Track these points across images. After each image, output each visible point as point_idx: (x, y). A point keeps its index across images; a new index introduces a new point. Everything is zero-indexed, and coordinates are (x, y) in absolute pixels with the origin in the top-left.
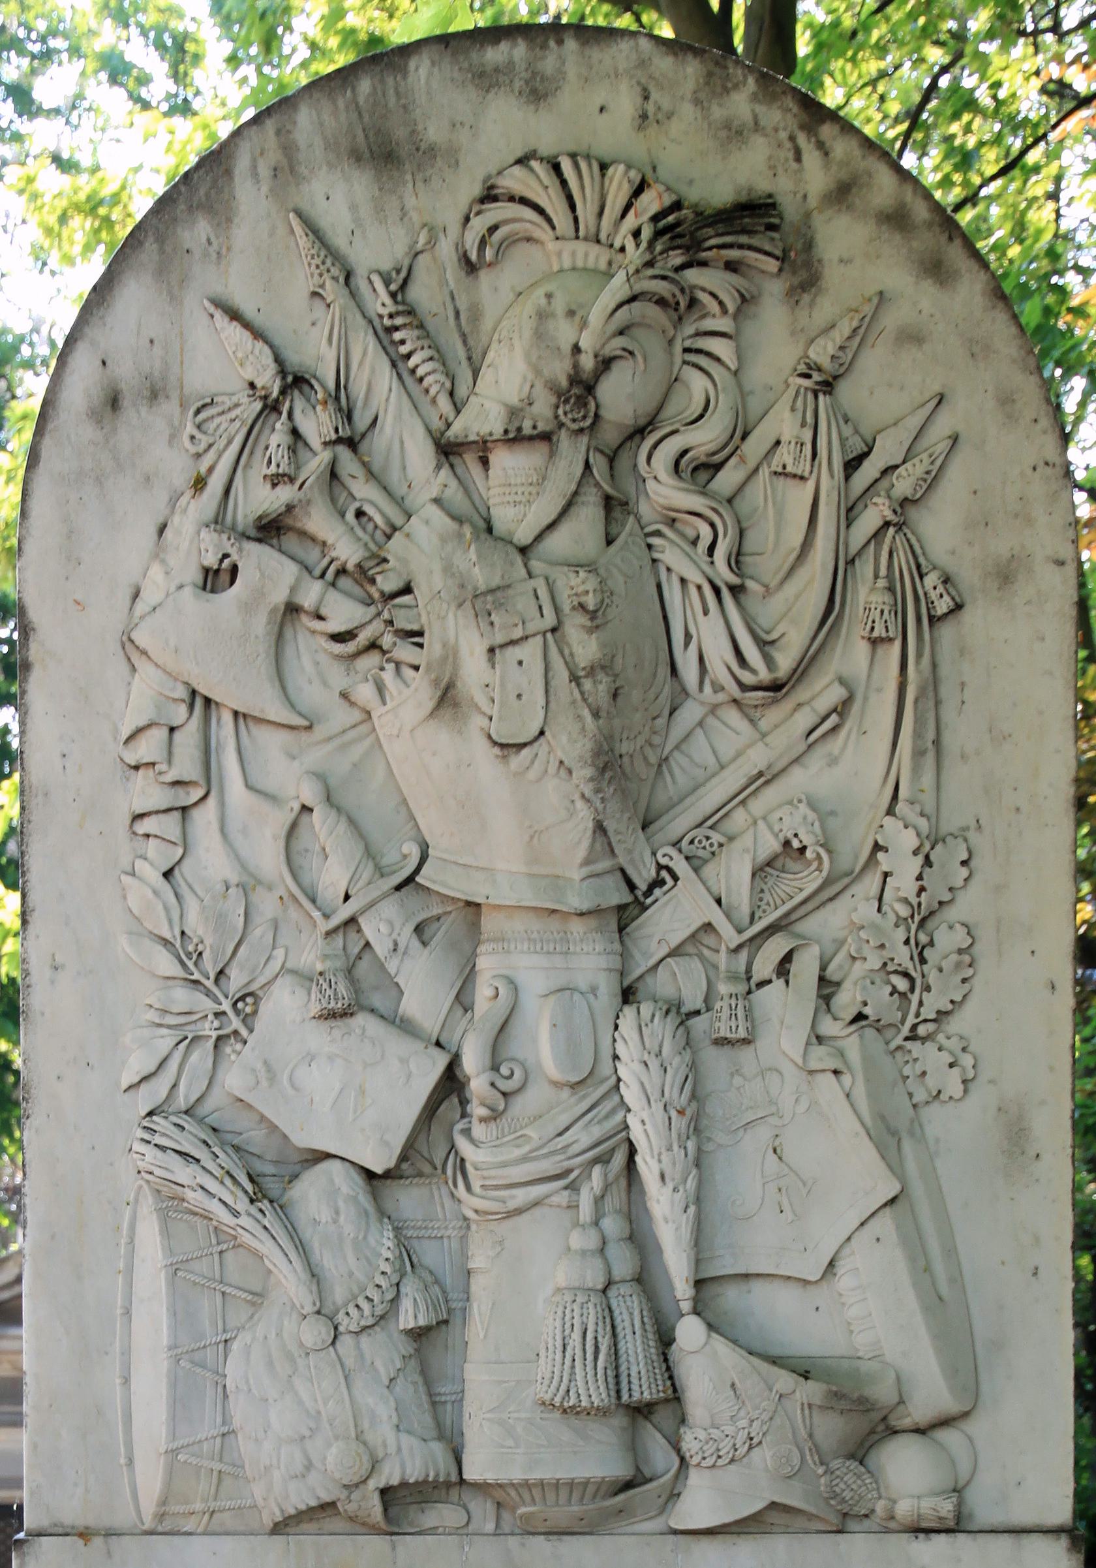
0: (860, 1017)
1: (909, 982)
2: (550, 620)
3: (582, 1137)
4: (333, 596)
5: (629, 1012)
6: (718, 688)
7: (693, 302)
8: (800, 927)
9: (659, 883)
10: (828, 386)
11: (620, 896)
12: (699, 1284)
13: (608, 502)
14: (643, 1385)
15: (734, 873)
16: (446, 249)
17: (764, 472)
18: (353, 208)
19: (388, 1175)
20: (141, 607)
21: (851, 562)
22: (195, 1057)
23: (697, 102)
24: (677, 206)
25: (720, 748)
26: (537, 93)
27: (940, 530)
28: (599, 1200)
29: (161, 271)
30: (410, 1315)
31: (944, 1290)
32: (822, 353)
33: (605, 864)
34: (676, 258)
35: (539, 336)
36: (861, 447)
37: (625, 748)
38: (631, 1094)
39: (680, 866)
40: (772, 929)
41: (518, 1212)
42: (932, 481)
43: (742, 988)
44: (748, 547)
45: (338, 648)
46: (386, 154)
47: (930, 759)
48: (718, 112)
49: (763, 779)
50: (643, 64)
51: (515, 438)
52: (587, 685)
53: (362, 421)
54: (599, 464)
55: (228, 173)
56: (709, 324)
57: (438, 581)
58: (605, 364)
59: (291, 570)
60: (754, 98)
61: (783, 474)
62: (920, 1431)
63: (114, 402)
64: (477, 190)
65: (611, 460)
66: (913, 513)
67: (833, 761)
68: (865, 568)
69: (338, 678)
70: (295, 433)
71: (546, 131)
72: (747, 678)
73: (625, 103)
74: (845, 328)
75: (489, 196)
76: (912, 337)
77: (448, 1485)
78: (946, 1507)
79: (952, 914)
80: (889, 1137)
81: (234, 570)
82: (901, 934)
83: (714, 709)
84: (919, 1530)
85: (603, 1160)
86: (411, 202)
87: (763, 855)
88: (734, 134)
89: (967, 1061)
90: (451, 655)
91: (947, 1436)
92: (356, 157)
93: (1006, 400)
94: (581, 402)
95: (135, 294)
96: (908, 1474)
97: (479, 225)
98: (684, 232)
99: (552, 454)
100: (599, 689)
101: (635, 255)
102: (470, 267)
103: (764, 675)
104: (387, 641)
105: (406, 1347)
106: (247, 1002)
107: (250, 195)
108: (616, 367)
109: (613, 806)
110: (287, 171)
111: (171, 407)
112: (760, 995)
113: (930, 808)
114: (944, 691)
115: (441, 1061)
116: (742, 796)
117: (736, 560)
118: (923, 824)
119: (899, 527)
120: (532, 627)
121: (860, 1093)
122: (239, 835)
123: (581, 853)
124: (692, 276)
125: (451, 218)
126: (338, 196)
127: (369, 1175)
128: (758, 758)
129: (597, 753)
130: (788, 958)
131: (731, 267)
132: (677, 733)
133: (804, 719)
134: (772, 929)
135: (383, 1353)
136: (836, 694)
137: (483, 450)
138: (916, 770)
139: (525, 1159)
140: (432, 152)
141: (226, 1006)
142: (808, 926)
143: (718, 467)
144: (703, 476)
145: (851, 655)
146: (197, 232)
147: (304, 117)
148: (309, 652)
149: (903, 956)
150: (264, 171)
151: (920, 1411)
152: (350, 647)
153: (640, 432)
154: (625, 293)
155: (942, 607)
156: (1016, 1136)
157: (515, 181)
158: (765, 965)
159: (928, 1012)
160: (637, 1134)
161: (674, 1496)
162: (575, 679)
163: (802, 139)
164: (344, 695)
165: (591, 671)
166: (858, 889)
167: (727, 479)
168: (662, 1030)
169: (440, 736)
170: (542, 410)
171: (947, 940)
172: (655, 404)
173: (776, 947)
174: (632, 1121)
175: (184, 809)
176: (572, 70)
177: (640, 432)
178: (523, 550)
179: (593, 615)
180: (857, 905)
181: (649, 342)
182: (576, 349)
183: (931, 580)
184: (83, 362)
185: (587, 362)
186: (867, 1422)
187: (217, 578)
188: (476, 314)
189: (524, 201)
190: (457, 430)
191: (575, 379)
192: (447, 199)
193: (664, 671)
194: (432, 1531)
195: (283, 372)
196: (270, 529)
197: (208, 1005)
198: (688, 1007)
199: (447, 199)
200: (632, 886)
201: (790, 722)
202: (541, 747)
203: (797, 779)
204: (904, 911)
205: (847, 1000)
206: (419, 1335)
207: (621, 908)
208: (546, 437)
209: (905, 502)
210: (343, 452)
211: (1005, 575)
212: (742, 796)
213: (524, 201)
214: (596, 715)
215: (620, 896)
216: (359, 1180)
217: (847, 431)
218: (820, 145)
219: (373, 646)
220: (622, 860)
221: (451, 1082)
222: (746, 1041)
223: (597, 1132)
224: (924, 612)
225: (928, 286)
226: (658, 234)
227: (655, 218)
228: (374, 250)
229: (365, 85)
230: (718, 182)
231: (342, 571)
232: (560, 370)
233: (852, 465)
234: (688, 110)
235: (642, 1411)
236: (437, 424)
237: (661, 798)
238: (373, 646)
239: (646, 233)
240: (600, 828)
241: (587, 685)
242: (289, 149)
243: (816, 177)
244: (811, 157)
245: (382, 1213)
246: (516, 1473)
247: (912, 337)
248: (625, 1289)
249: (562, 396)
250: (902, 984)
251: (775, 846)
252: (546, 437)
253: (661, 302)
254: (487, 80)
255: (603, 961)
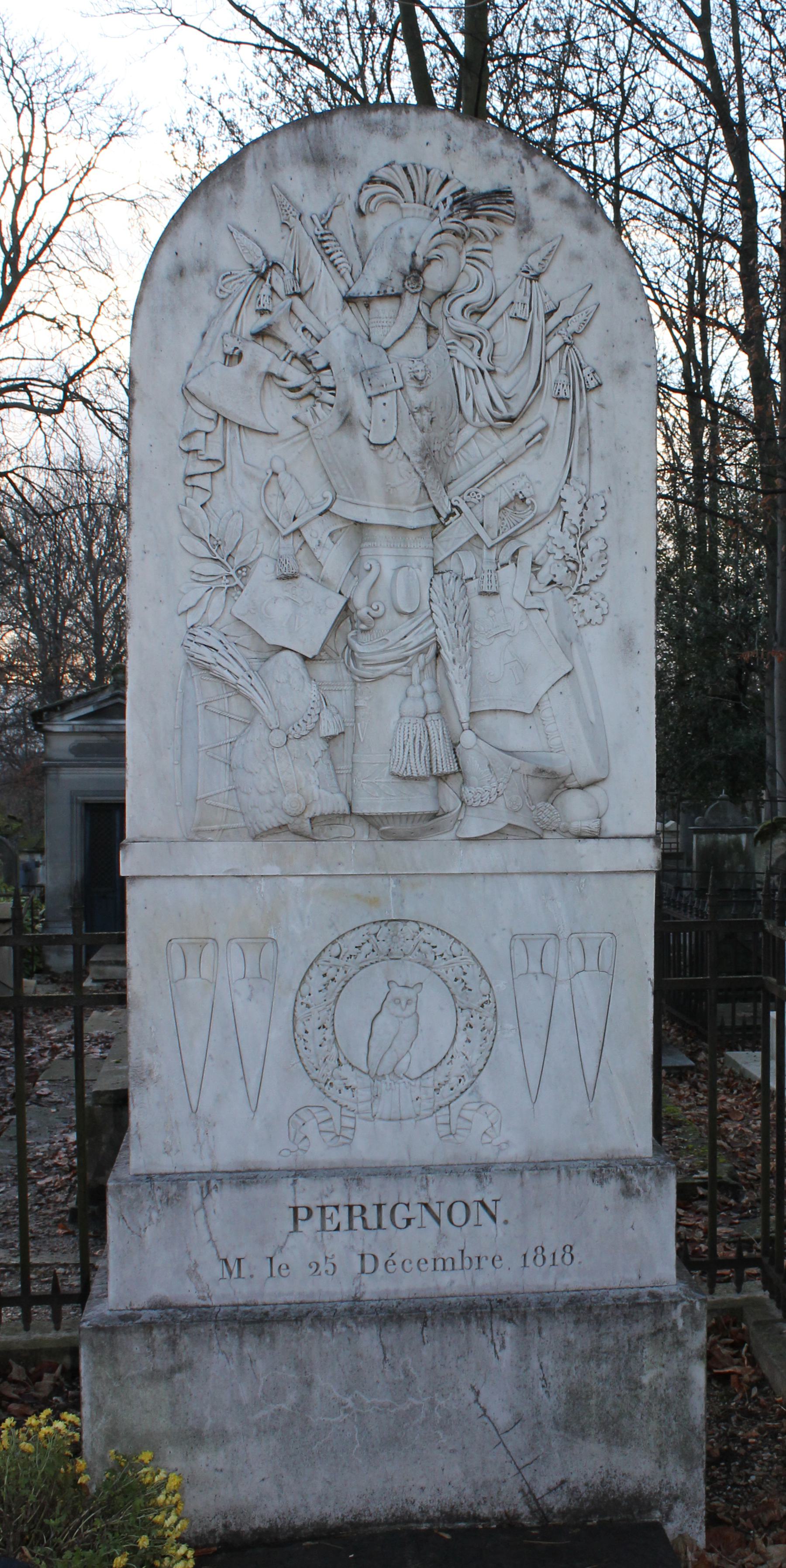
0: (552, 582)
1: (575, 565)
2: (400, 384)
3: (413, 640)
4: (290, 368)
5: (438, 578)
6: (482, 418)
7: (471, 235)
8: (522, 538)
9: (454, 514)
10: (537, 277)
11: (432, 520)
12: (472, 714)
13: (429, 328)
14: (446, 766)
15: (491, 510)
16: (349, 206)
17: (506, 317)
18: (304, 184)
19: (314, 659)
20: (192, 372)
21: (547, 361)
22: (215, 600)
23: (474, 143)
24: (464, 190)
25: (479, 449)
26: (396, 134)
27: (589, 348)
28: (422, 671)
29: (207, 211)
30: (328, 727)
31: (593, 718)
32: (534, 262)
33: (427, 504)
34: (464, 213)
35: (396, 247)
36: (553, 307)
37: (436, 447)
38: (439, 619)
39: (464, 507)
40: (510, 537)
41: (381, 678)
42: (587, 324)
43: (493, 567)
44: (497, 352)
45: (292, 395)
46: (320, 159)
47: (586, 458)
48: (483, 148)
49: (504, 464)
50: (447, 124)
51: (383, 296)
52: (418, 415)
53: (306, 285)
54: (424, 310)
55: (242, 165)
56: (479, 246)
57: (344, 363)
58: (428, 262)
59: (269, 356)
60: (502, 142)
61: (515, 318)
62: (581, 788)
63: (181, 272)
64: (366, 178)
65: (430, 308)
66: (578, 339)
67: (539, 457)
68: (554, 365)
69: (293, 409)
70: (272, 289)
71: (401, 153)
72: (497, 414)
73: (438, 142)
74: (545, 250)
75: (372, 180)
76: (577, 257)
77: (344, 815)
78: (594, 825)
79: (596, 533)
80: (567, 642)
81: (240, 355)
82: (572, 542)
83: (480, 429)
84: (581, 837)
85: (424, 652)
86: (332, 182)
87: (504, 502)
88: (492, 159)
89: (603, 605)
90: (348, 400)
91: (592, 790)
92: (306, 160)
93: (622, 289)
94: (417, 280)
95: (193, 222)
96: (577, 808)
97: (366, 194)
98: (467, 202)
99: (401, 304)
100: (425, 418)
101: (444, 212)
102: (361, 213)
103: (506, 414)
104: (317, 392)
105: (323, 745)
106: (244, 569)
107: (252, 176)
108: (433, 263)
109: (430, 476)
110: (271, 166)
111: (211, 276)
112: (502, 571)
113: (586, 481)
114: (592, 425)
115: (342, 601)
116: (493, 472)
117: (492, 357)
118: (583, 490)
119: (571, 345)
120: (389, 388)
121: (552, 619)
122: (237, 500)
123: (414, 499)
124: (471, 222)
125: (354, 193)
126: (297, 180)
127: (305, 658)
128: (503, 453)
129: (423, 449)
130: (516, 553)
131: (490, 219)
132: (459, 443)
133: (526, 436)
134: (510, 537)
135: (315, 747)
136: (540, 424)
137: (368, 301)
138: (580, 463)
139: (384, 651)
140: (344, 159)
141: (232, 572)
142: (526, 538)
143: (483, 313)
144: (476, 317)
145: (546, 407)
146: (224, 192)
147: (281, 139)
148: (276, 397)
149: (573, 553)
150: (260, 166)
151: (582, 778)
152: (298, 395)
153: (444, 295)
154: (439, 229)
155: (592, 384)
156: (628, 644)
157: (383, 174)
158: (505, 556)
159: (585, 581)
160: (441, 637)
161: (458, 821)
162: (412, 413)
163: (524, 162)
164: (295, 418)
165: (420, 409)
166: (551, 519)
167: (486, 320)
168: (453, 587)
169: (344, 439)
170: (396, 284)
171: (594, 546)
172: (452, 282)
173: (512, 546)
174: (440, 632)
175: (212, 473)
176: (413, 125)
177: (444, 295)
178: (386, 350)
179: (421, 382)
180: (551, 526)
181: (449, 252)
182: (414, 254)
183: (587, 371)
184: (166, 254)
185: (419, 261)
186: (556, 783)
187: (233, 357)
188: (364, 237)
189: (389, 184)
190: (354, 291)
191: (412, 269)
192: (349, 183)
193: (455, 410)
194: (338, 838)
195: (267, 261)
196: (260, 335)
197: (223, 571)
198: (468, 575)
199: (349, 183)
200: (439, 516)
201: (514, 439)
202: (394, 446)
203: (519, 467)
204: (574, 531)
205: (545, 575)
206: (329, 739)
207: (433, 526)
208: (399, 296)
209: (575, 333)
210: (296, 299)
211: (623, 371)
212: (493, 472)
213: (389, 184)
214: (422, 430)
215: (432, 520)
216: (299, 660)
217: (546, 299)
218: (533, 166)
219: (310, 394)
220: (435, 503)
221: (347, 611)
222: (496, 594)
223: (421, 638)
224: (582, 386)
225: (585, 234)
226: (455, 203)
227: (453, 195)
228: (314, 204)
229: (311, 127)
230: (482, 184)
231: (295, 357)
232: (406, 264)
233: (549, 315)
234: (469, 146)
235: (442, 778)
236: (344, 288)
237: (453, 472)
238: (310, 394)
239: (450, 201)
240: (424, 486)
241: (418, 415)
242: (273, 156)
243: (531, 180)
244: (529, 170)
245: (311, 678)
246: (380, 810)
247: (577, 257)
248: (435, 717)
249: (405, 277)
250: (573, 566)
251: (512, 496)
252: (399, 296)
253: (456, 234)
254: (371, 127)
255: (424, 553)
